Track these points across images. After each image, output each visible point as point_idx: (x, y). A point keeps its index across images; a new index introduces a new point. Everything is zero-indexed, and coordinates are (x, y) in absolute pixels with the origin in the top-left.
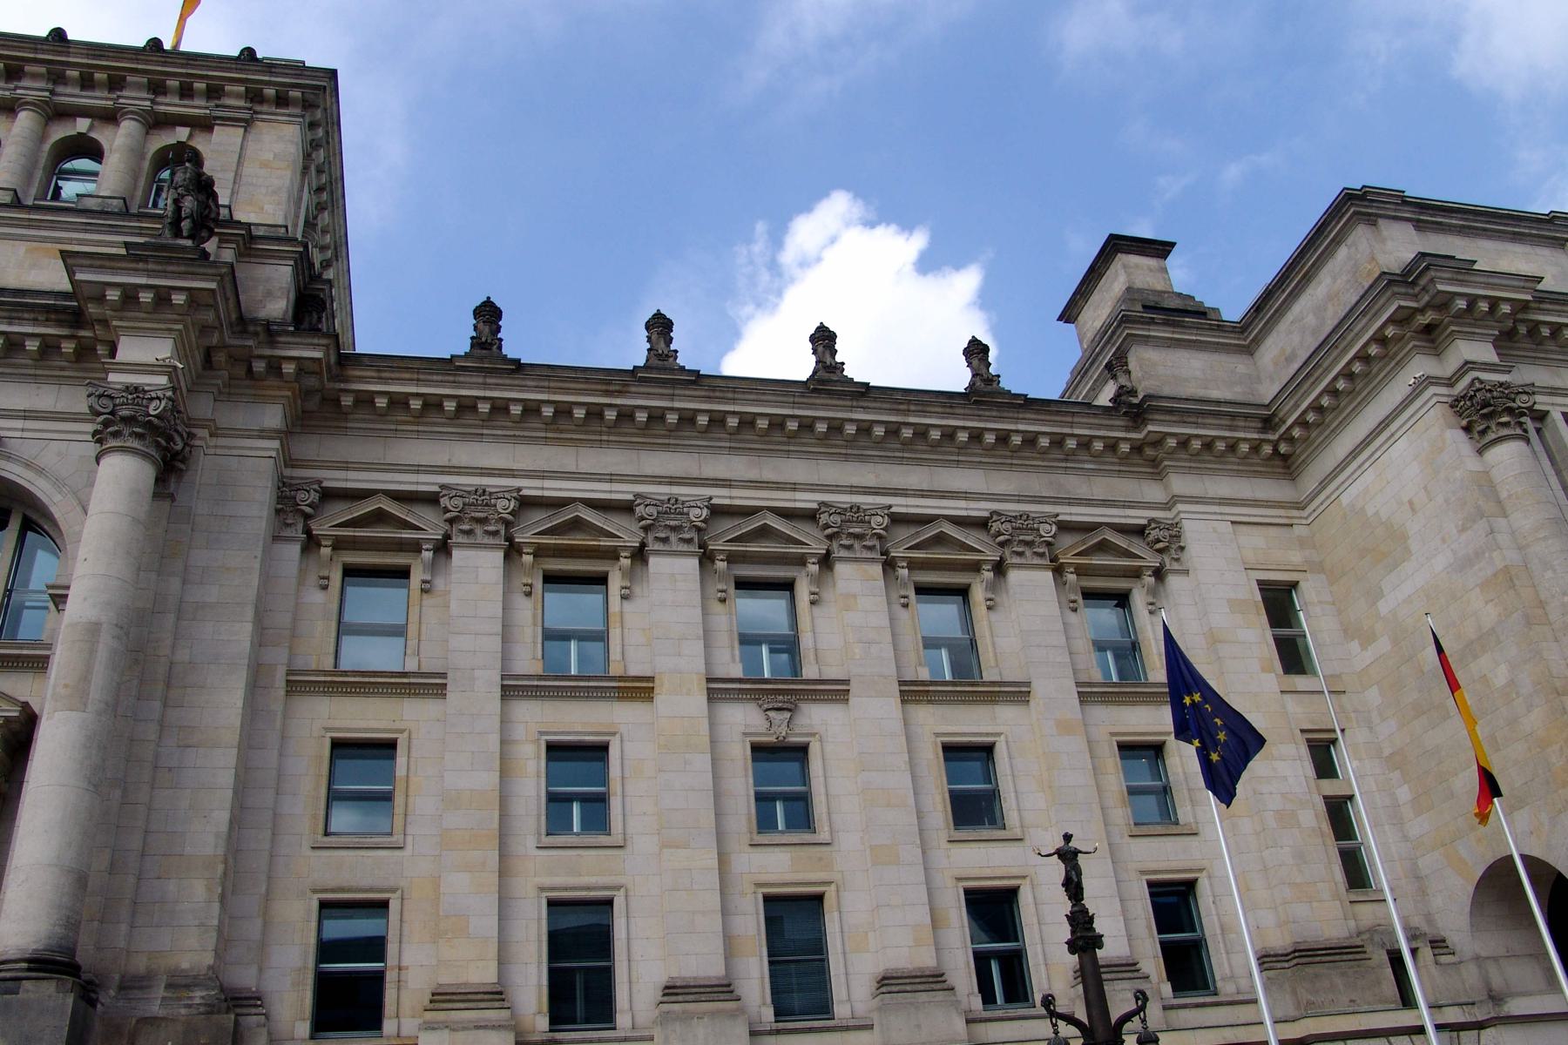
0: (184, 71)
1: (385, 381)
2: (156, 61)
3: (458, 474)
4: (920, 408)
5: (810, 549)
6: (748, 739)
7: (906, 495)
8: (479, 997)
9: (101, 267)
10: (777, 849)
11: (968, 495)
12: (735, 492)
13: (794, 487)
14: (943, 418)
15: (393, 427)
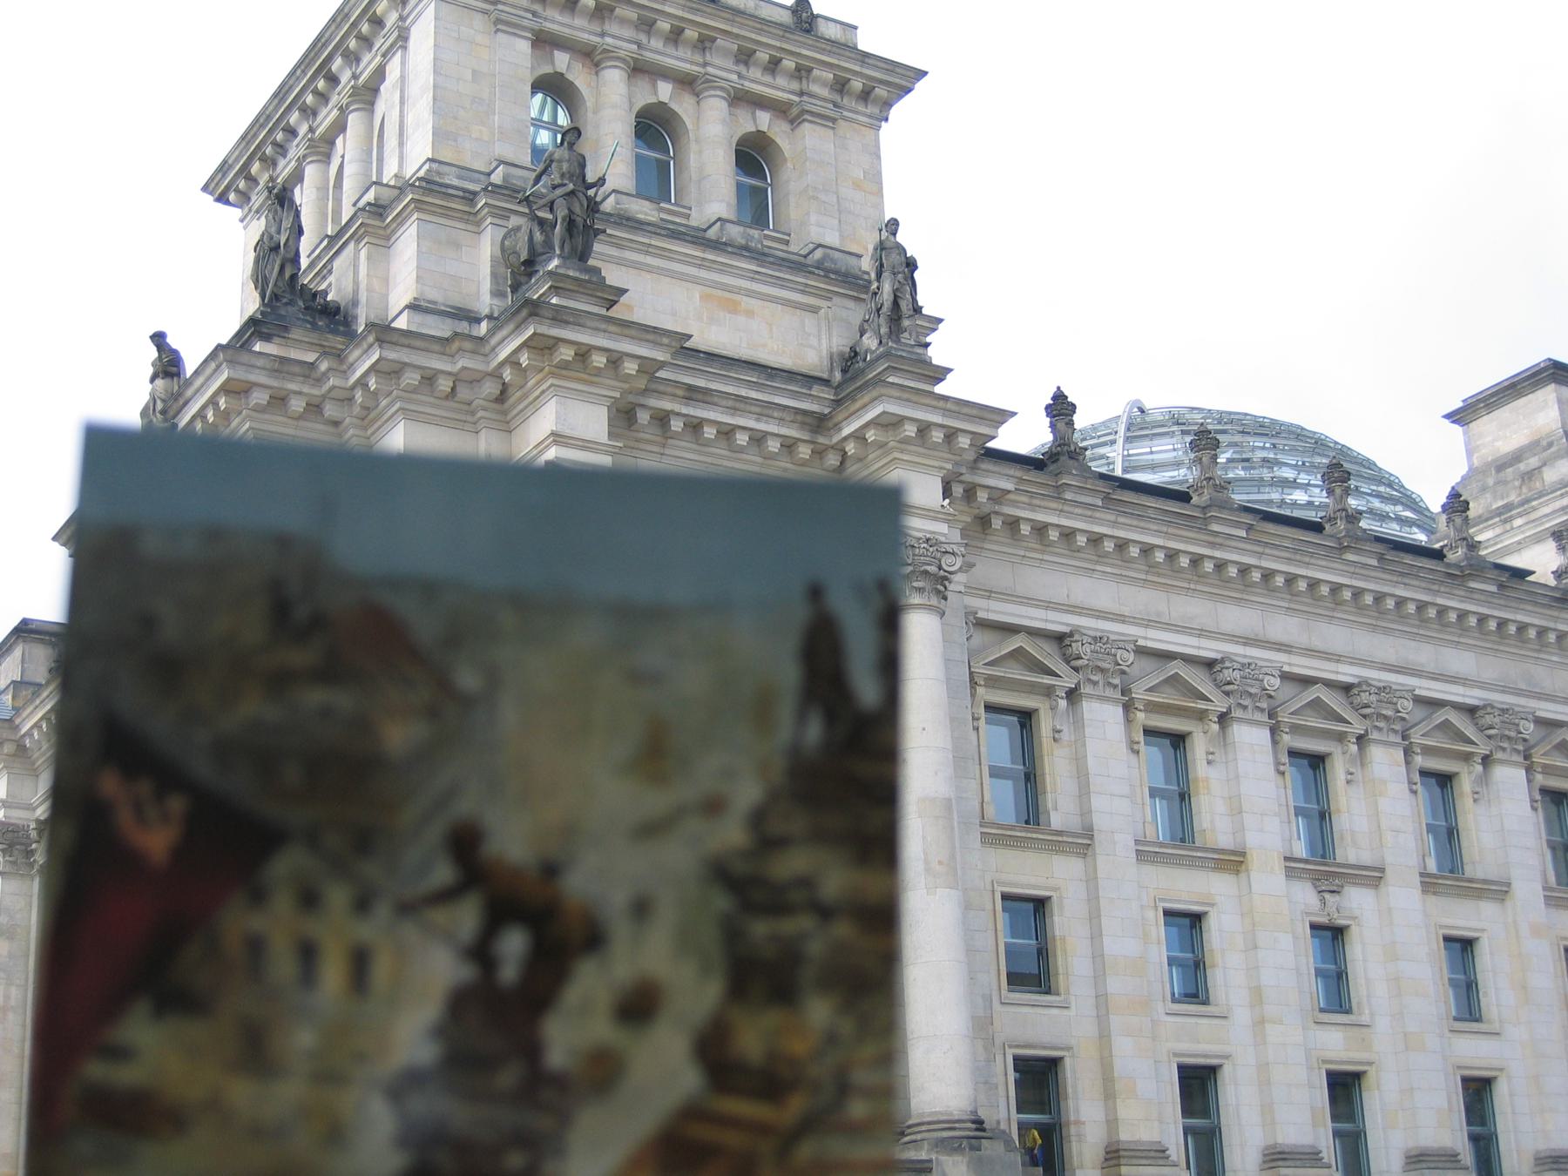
0: (778, 44)
1: (1032, 507)
2: (754, 27)
3: (1080, 614)
4: (1447, 590)
5: (1351, 728)
6: (1309, 918)
7: (1420, 676)
8: (1153, 1154)
9: (908, 400)
10: (1333, 1028)
11: (1467, 682)
12: (1295, 659)
13: (1337, 658)
14: (1462, 601)
15: (1022, 553)
